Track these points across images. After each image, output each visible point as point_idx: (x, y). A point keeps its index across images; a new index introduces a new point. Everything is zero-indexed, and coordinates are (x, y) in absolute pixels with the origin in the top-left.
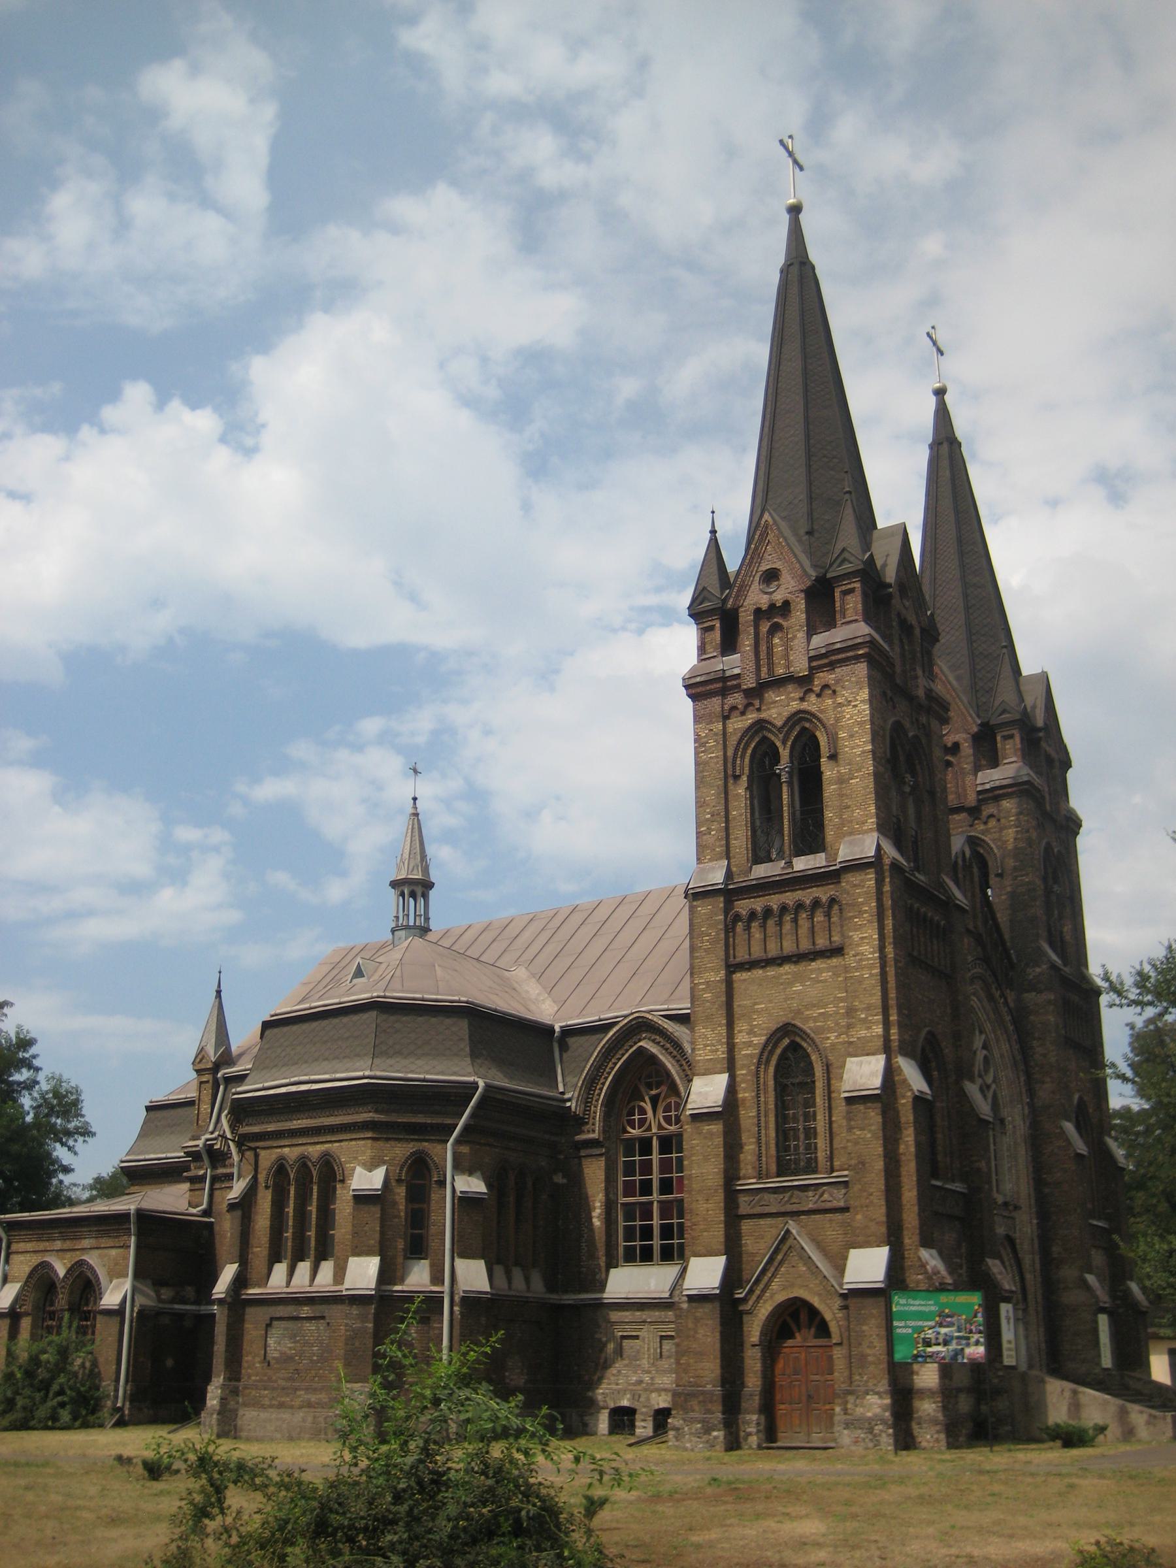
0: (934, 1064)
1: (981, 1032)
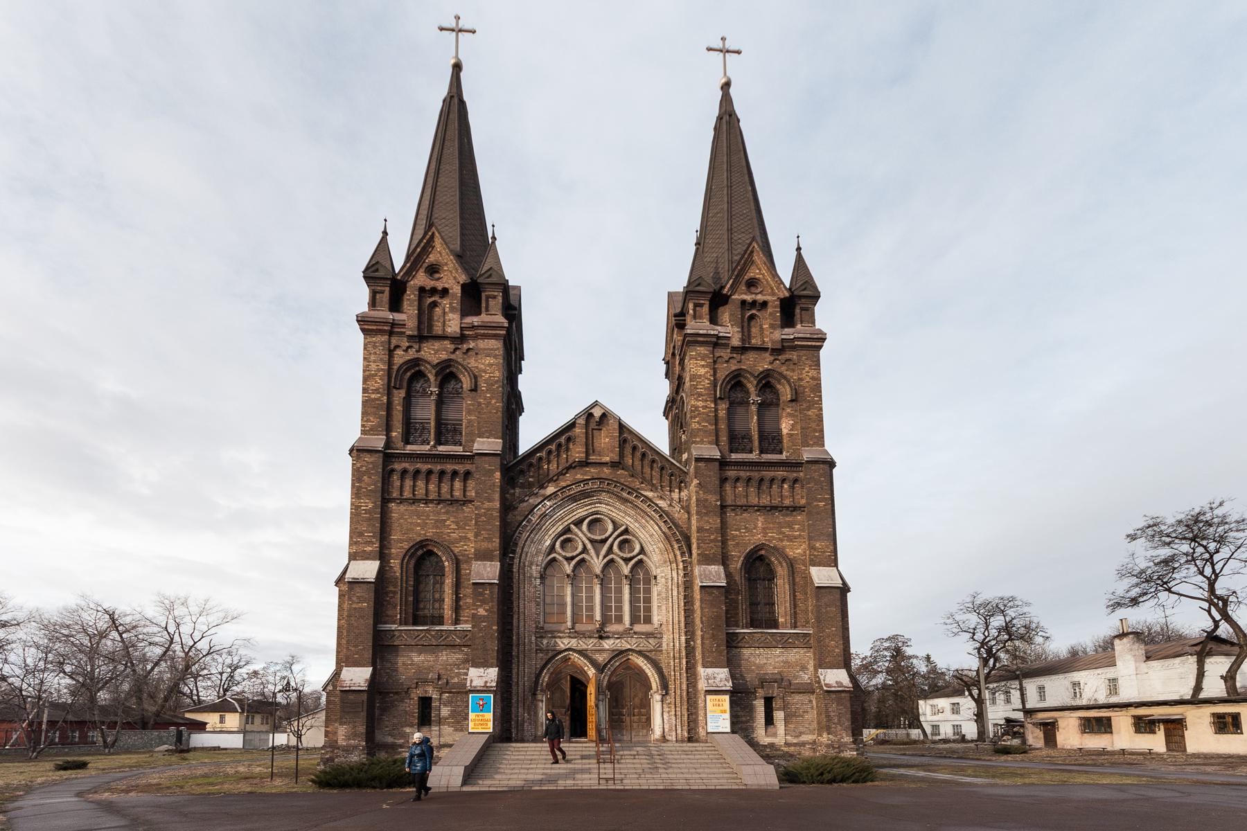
0: (444, 559)
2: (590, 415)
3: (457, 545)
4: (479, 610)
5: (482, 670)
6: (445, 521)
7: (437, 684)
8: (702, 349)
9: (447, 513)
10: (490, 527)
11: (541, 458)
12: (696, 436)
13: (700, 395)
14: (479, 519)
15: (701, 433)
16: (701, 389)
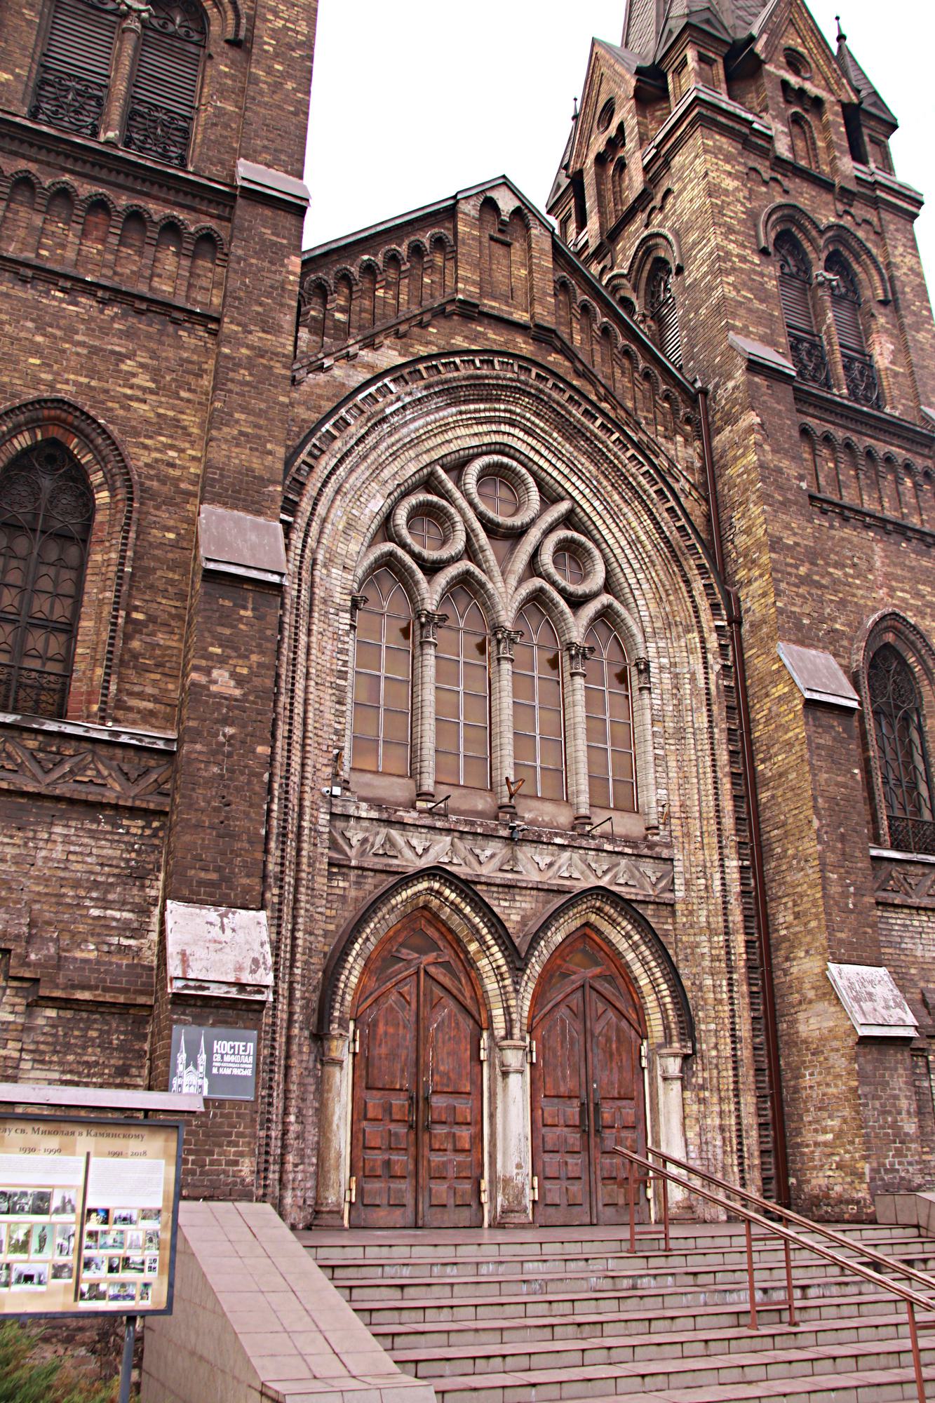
0: (97, 478)
1: (549, 497)
2: (490, 205)
4: (215, 673)
5: (211, 914)
6: (121, 357)
7: (25, 962)
8: (724, 140)
9: (128, 334)
10: (263, 406)
11: (369, 269)
13: (730, 230)
14: (231, 375)
15: (742, 312)
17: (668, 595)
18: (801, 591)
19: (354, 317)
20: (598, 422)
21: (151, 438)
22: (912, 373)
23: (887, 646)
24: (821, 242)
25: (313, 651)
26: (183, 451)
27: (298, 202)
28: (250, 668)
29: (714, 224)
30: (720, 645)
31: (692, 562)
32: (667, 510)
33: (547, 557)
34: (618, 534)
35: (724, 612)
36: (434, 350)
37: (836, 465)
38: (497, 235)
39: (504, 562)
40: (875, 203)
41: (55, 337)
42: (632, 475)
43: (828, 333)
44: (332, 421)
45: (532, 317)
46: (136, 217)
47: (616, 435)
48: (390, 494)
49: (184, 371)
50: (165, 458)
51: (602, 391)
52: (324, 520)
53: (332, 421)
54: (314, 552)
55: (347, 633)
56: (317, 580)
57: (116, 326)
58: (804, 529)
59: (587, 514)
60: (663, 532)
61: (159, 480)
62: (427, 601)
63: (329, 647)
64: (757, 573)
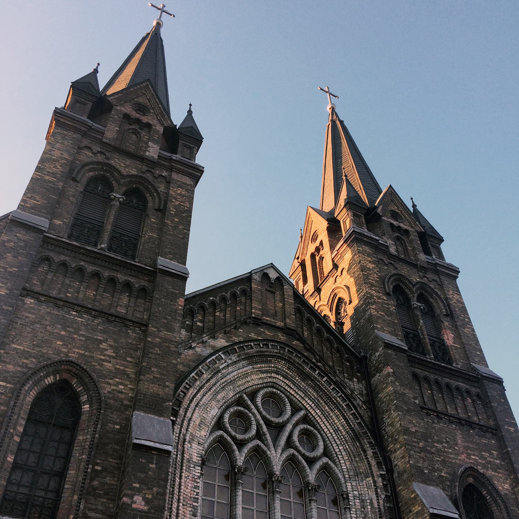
0: (84, 398)
1: (296, 409)
2: (266, 276)
3: (110, 381)
4: (136, 498)
6: (100, 342)
9: (103, 332)
11: (213, 304)
12: (377, 323)
13: (372, 285)
14: (151, 350)
16: (372, 280)
17: (355, 458)
18: (421, 455)
19: (206, 325)
20: (317, 372)
21: (112, 379)
22: (464, 348)
23: (470, 484)
24: (414, 289)
25: (182, 487)
26: (127, 385)
27: (184, 275)
28: (153, 495)
29: (365, 283)
30: (384, 484)
31: (366, 441)
32: (352, 414)
33: (295, 438)
34: (329, 427)
35: (384, 467)
36: (242, 339)
37: (432, 392)
38: (269, 289)
39: (275, 441)
40: (437, 272)
41: (70, 332)
42: (334, 397)
43: (421, 329)
44: (195, 372)
45: (285, 324)
46: (112, 280)
47: (326, 378)
48: (221, 407)
49: (129, 348)
50: (118, 389)
51: (318, 357)
52: (190, 420)
53: (195, 372)
54: (185, 435)
55: (199, 477)
56: (186, 449)
57: (99, 328)
58: (420, 424)
59: (314, 417)
60: (351, 425)
61: (114, 400)
62: (239, 461)
63: (190, 485)
64: (398, 446)
